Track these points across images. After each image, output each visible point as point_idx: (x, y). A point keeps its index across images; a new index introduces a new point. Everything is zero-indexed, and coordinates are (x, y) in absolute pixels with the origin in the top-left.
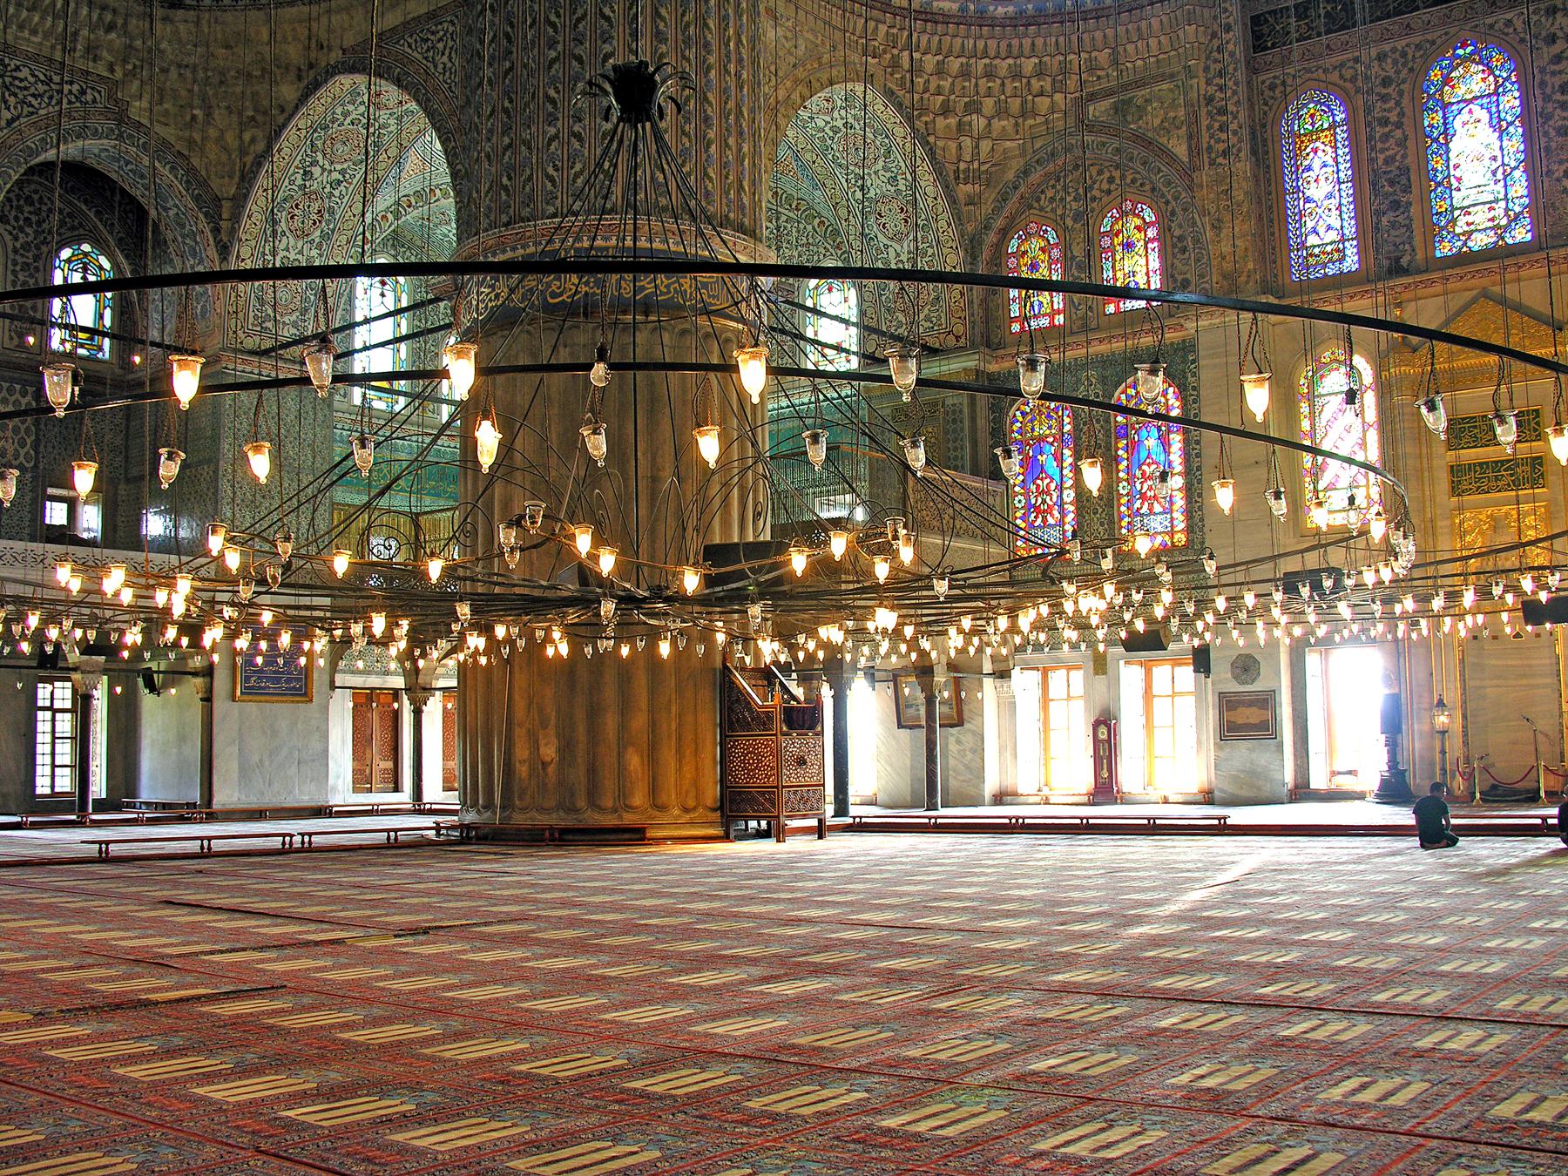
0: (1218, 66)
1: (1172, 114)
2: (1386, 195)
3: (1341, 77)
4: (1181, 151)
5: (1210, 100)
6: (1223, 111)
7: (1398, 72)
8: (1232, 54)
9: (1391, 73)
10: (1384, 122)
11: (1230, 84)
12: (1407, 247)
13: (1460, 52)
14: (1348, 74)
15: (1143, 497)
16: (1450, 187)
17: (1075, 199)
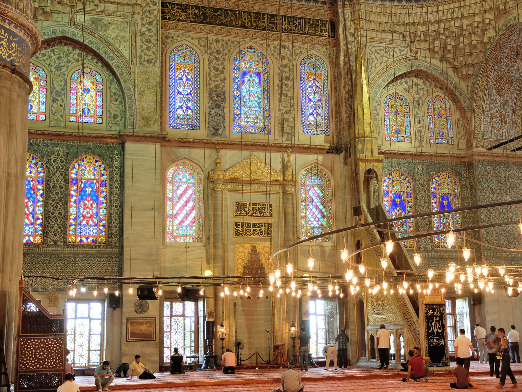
0: (148, 20)
1: (122, 34)
2: (215, 101)
3: (199, 44)
4: (126, 53)
5: (142, 34)
6: (149, 41)
7: (223, 50)
8: (156, 17)
9: (221, 50)
10: (216, 69)
11: (154, 30)
12: (222, 125)
13: (250, 50)
14: (202, 43)
15: (84, 217)
16: (239, 106)
17: (58, 58)
